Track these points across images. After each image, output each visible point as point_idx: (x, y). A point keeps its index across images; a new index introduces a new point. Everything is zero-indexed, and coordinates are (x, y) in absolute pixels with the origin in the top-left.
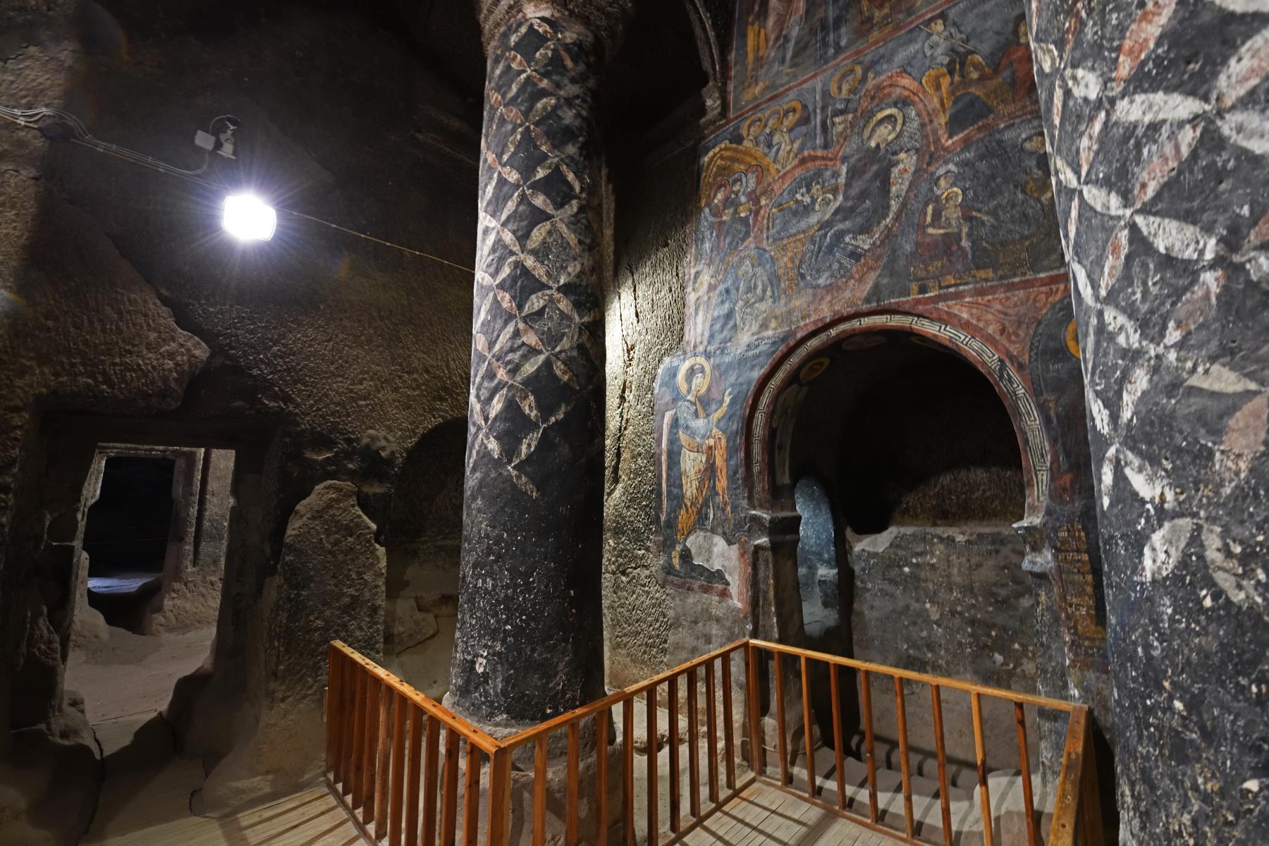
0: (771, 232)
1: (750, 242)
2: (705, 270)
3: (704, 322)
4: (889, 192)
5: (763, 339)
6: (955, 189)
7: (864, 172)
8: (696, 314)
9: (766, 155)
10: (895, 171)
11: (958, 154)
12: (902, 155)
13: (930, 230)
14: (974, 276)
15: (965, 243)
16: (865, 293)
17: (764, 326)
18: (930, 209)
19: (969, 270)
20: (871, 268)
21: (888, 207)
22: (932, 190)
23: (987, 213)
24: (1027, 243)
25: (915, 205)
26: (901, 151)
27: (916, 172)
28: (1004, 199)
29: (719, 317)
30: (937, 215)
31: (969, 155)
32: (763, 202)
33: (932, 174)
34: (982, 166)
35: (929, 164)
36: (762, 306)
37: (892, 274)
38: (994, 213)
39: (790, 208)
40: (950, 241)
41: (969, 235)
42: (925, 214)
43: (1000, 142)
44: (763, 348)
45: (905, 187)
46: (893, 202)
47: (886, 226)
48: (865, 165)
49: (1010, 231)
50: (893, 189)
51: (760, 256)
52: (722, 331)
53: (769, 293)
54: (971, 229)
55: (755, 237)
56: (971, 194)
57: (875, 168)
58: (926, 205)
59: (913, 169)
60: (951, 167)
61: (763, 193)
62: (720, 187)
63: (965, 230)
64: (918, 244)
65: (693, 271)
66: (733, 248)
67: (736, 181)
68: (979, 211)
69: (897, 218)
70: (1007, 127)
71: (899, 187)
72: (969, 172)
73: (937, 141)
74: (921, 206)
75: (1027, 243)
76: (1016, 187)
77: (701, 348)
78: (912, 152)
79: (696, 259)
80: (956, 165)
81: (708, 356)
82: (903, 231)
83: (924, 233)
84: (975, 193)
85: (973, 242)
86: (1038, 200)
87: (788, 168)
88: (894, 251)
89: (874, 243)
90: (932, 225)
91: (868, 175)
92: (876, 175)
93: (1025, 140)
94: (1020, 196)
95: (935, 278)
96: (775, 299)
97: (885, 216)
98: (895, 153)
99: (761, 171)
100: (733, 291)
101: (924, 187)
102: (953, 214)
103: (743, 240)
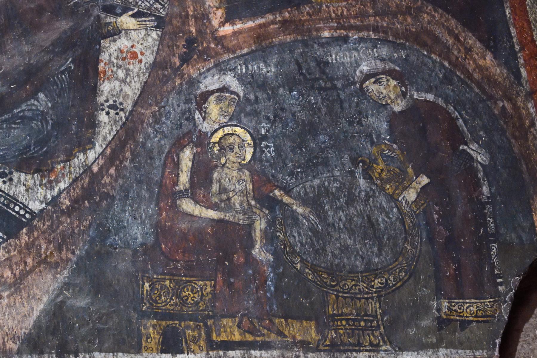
4: (94, 90)
6: (239, 130)
7: (37, 27)
10: (111, 50)
11: (246, 59)
12: (127, 21)
13: (187, 205)
14: (280, 333)
15: (260, 252)
16: (30, 322)
18: (187, 156)
19: (271, 315)
20: (44, 261)
21: (94, 124)
22: (191, 119)
23: (304, 201)
24: (377, 282)
25: (155, 139)
26: (125, 10)
27: (155, 66)
28: (332, 178)
30: (202, 173)
31: (268, 69)
33: (193, 83)
34: (291, 99)
35: (185, 59)
37: (98, 287)
38: (314, 202)
40: (228, 240)
41: (270, 238)
42: (177, 165)
43: (322, 64)
45: (132, 90)
46: (103, 117)
47: (88, 169)
48: (40, 10)
49: (345, 249)
50: (106, 87)
54: (271, 223)
56: (270, 152)
57: (64, 25)
58: (179, 145)
59: (150, 58)
60: (230, 80)
63: (260, 225)
64: (161, 231)
68: (288, 191)
69: (113, 157)
70: (334, 40)
71: (120, 84)
72: (266, 106)
73: (203, 17)
74: (167, 144)
75: (377, 282)
76: (355, 162)
78: (150, 22)
80: (241, 79)
82: (125, 190)
83: (174, 207)
84: (277, 149)
85: (275, 254)
86: (392, 198)
88: (104, 233)
89: (55, 202)
90: (191, 193)
91: (46, 37)
92: (65, 45)
93: (368, 76)
94: (362, 182)
95: (200, 319)
97: (84, 144)
98: (110, 10)
101: (174, 105)
102: (233, 179)
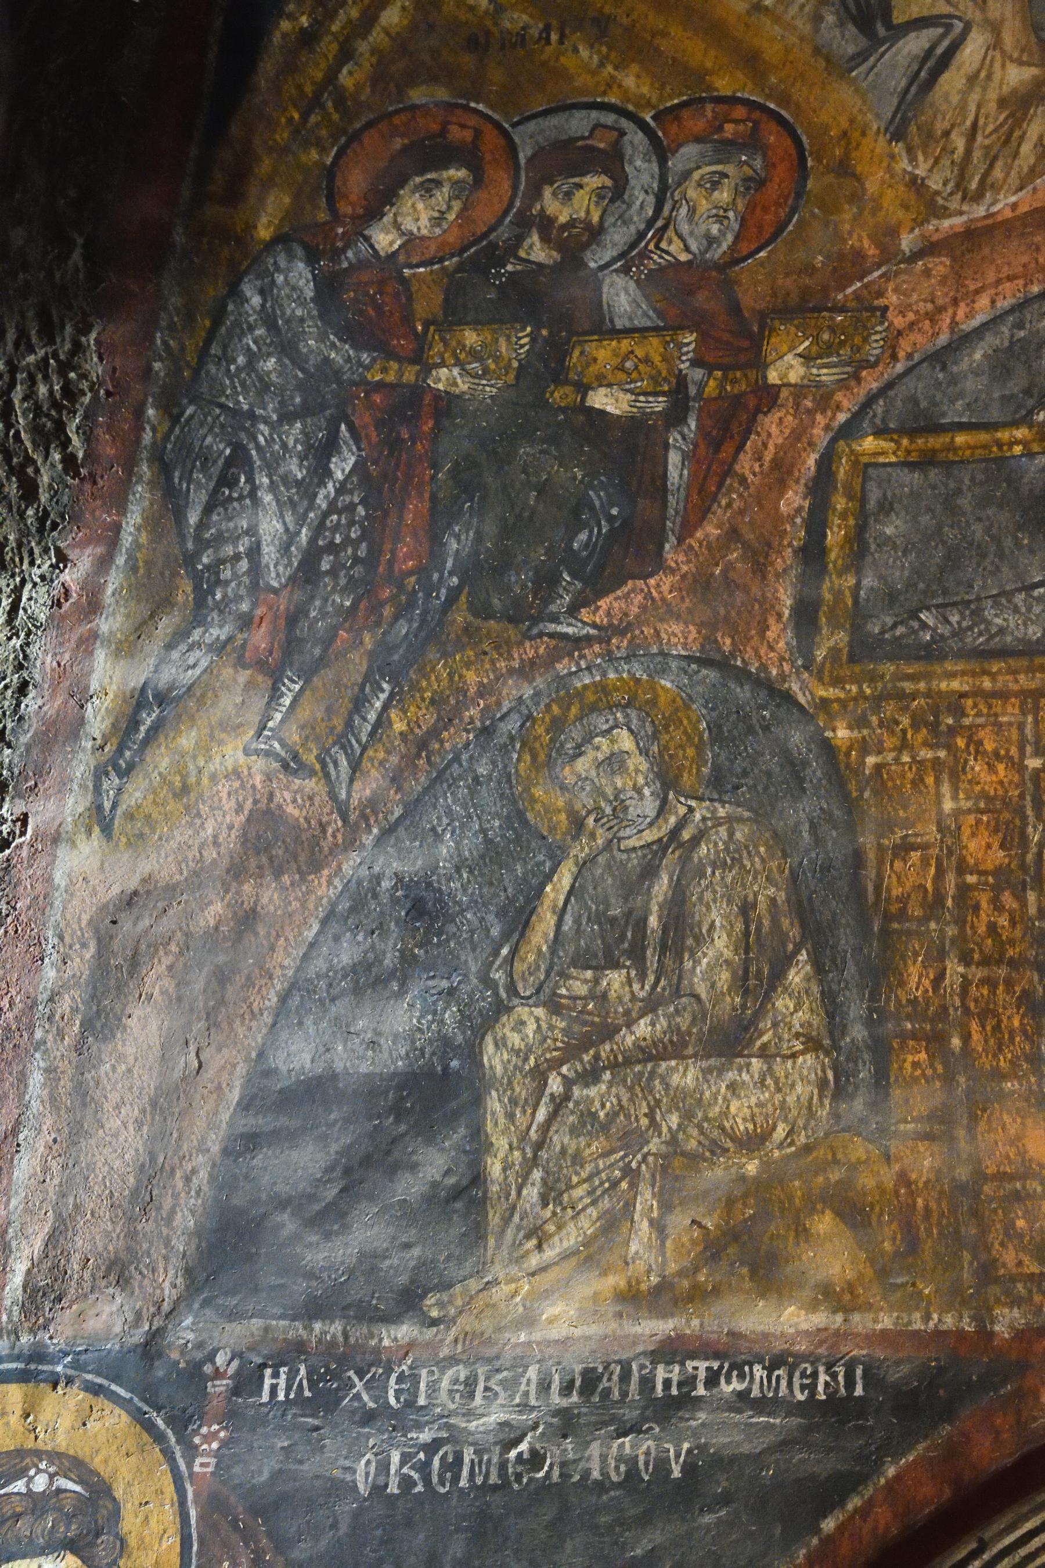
0: (837, 584)
1: (658, 613)
2: (236, 693)
3: (167, 1104)
5: (730, 1355)
8: (100, 1022)
9: (840, 68)
17: (748, 1246)
29: (315, 1091)
32: (787, 368)
36: (741, 1096)
39: (998, 466)
44: (718, 1429)
51: (729, 730)
52: (330, 1218)
53: (794, 1006)
55: (700, 585)
61: (803, 307)
62: (429, 155)
65: (108, 677)
66: (509, 600)
67: (568, 160)
77: (108, 1318)
79: (153, 598)
81: (161, 1390)
87: (1003, 203)
96: (859, 1064)
99: (791, 165)
100: (476, 920)
103: (600, 579)
